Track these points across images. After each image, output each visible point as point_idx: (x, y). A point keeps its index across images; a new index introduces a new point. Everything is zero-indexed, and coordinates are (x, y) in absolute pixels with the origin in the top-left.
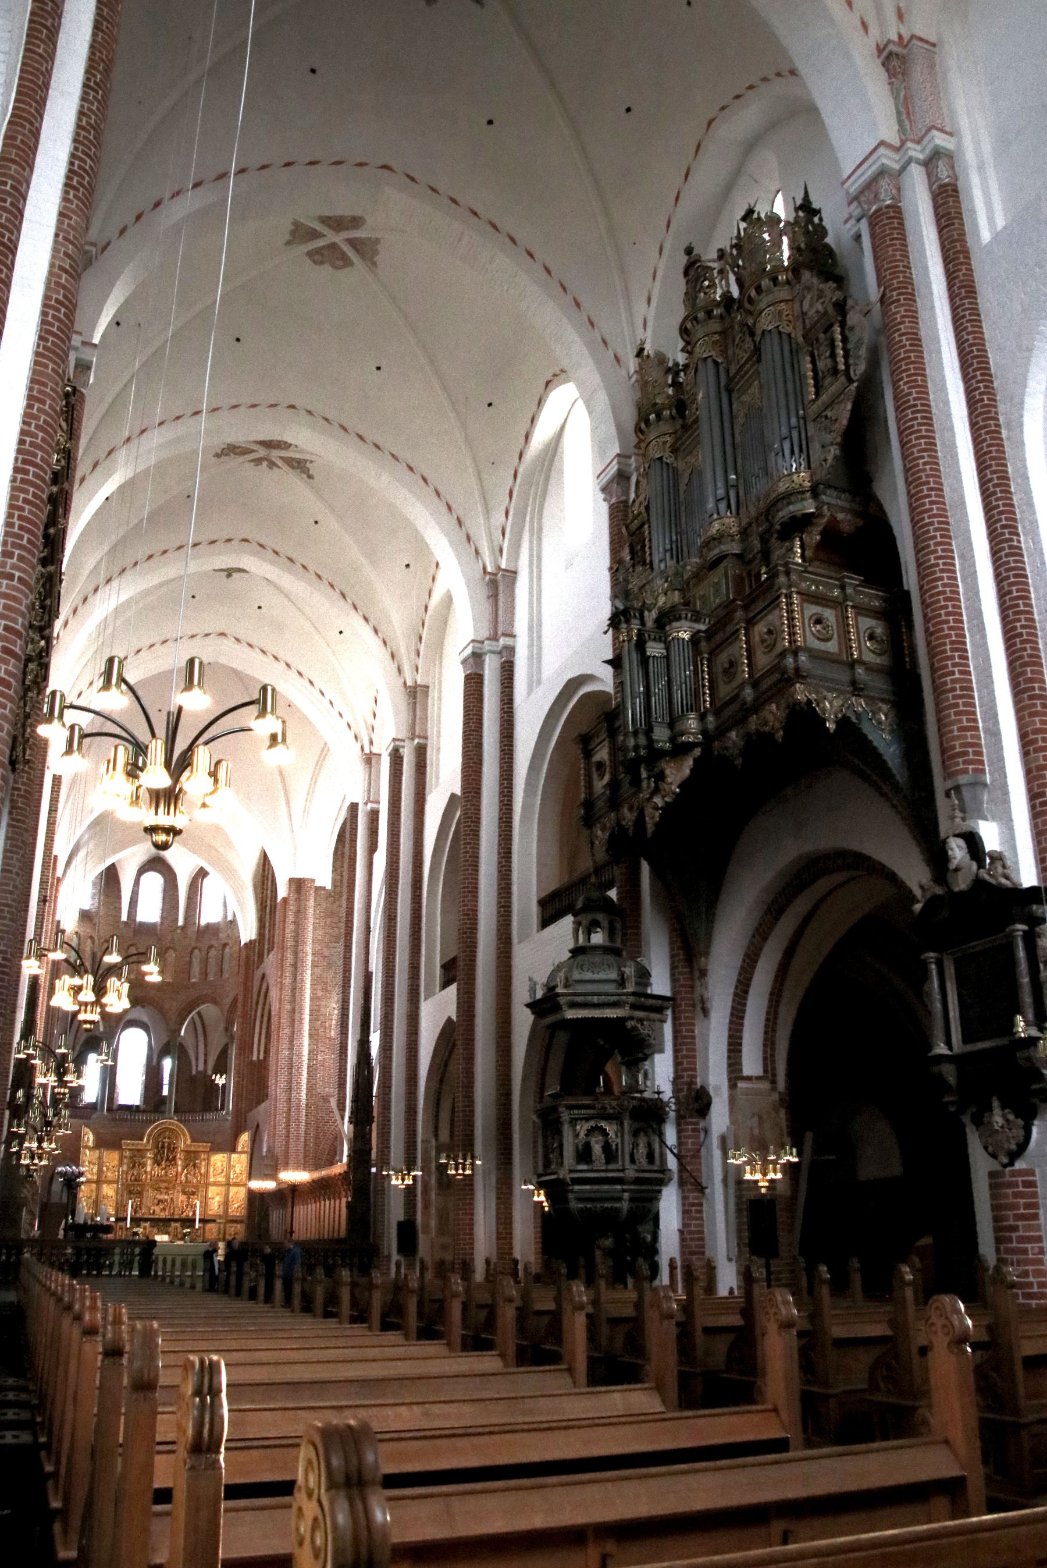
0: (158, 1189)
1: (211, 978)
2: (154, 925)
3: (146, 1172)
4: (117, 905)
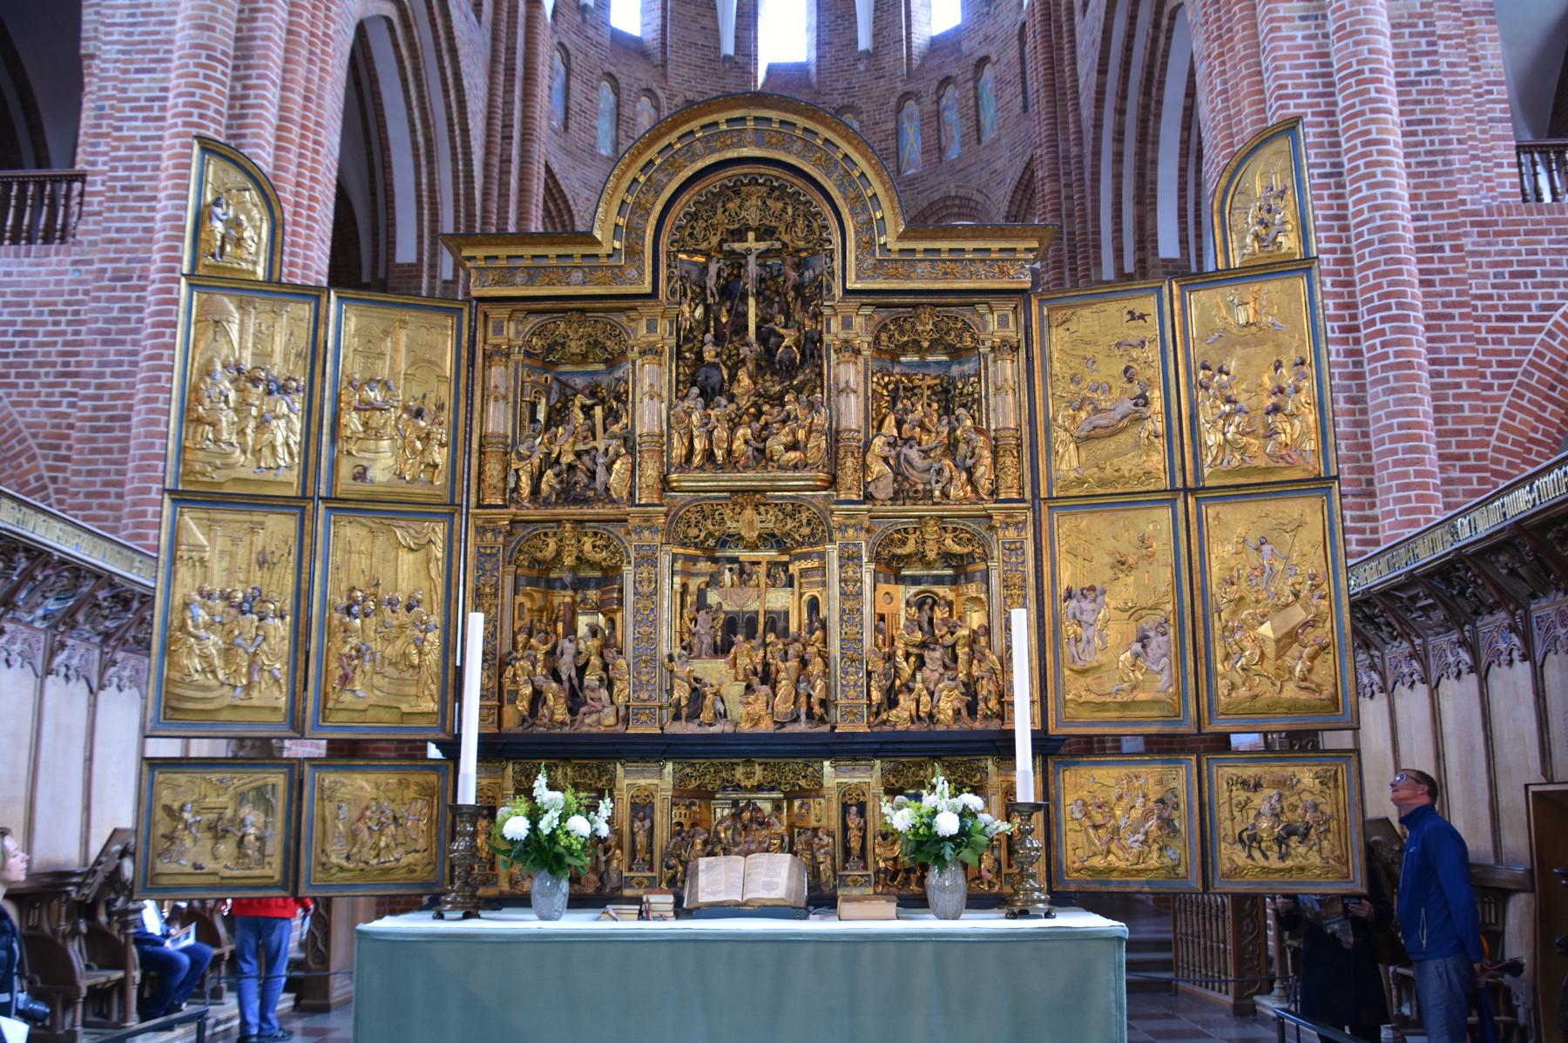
0: (716, 547)
1: (953, 153)
2: (801, 68)
3: (628, 440)
4: (706, 22)
